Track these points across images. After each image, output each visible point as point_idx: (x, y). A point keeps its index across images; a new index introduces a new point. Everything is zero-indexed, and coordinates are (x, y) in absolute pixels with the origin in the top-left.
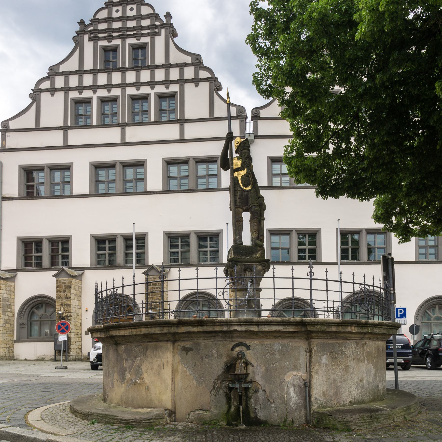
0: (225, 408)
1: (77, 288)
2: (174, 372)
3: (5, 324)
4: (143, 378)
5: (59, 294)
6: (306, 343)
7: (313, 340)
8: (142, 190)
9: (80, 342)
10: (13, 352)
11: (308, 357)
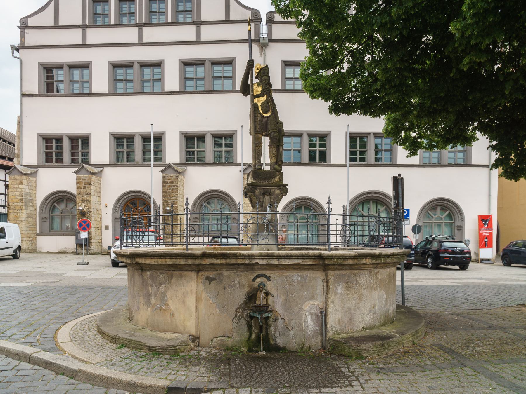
0: (246, 335)
1: (96, 184)
2: (198, 299)
3: (28, 218)
4: (168, 305)
5: (80, 190)
6: (324, 274)
7: (330, 271)
8: (160, 90)
9: (101, 237)
10: (36, 245)
11: (325, 287)
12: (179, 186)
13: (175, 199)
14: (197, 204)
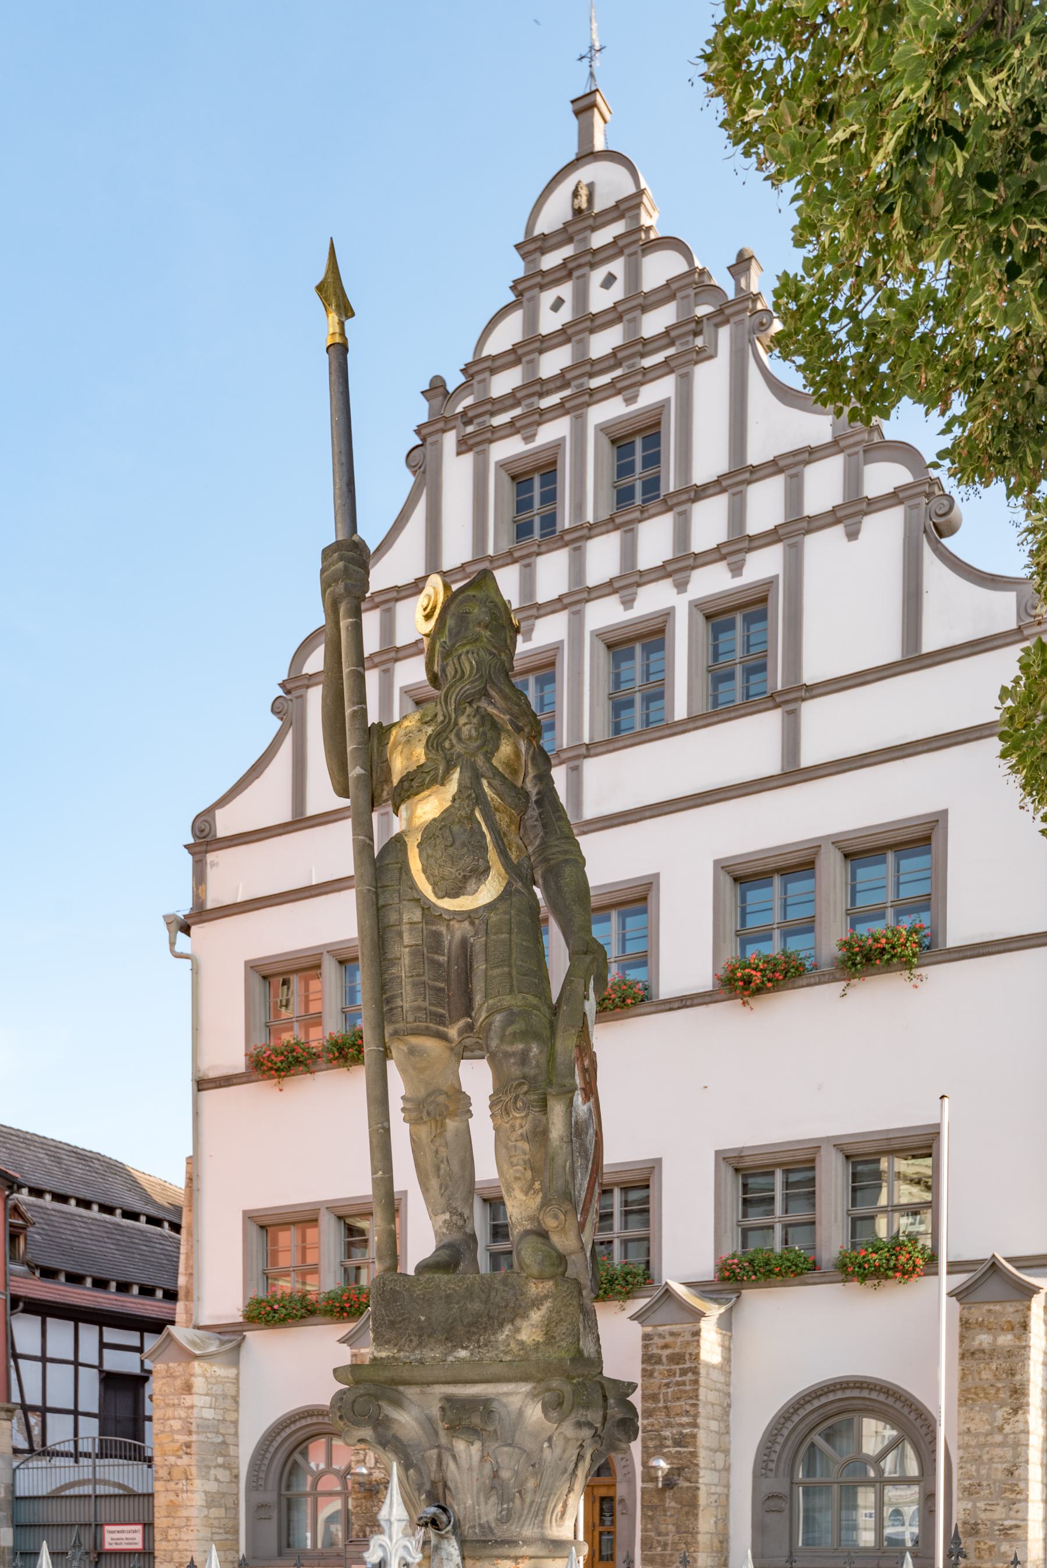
13: (689, 1425)
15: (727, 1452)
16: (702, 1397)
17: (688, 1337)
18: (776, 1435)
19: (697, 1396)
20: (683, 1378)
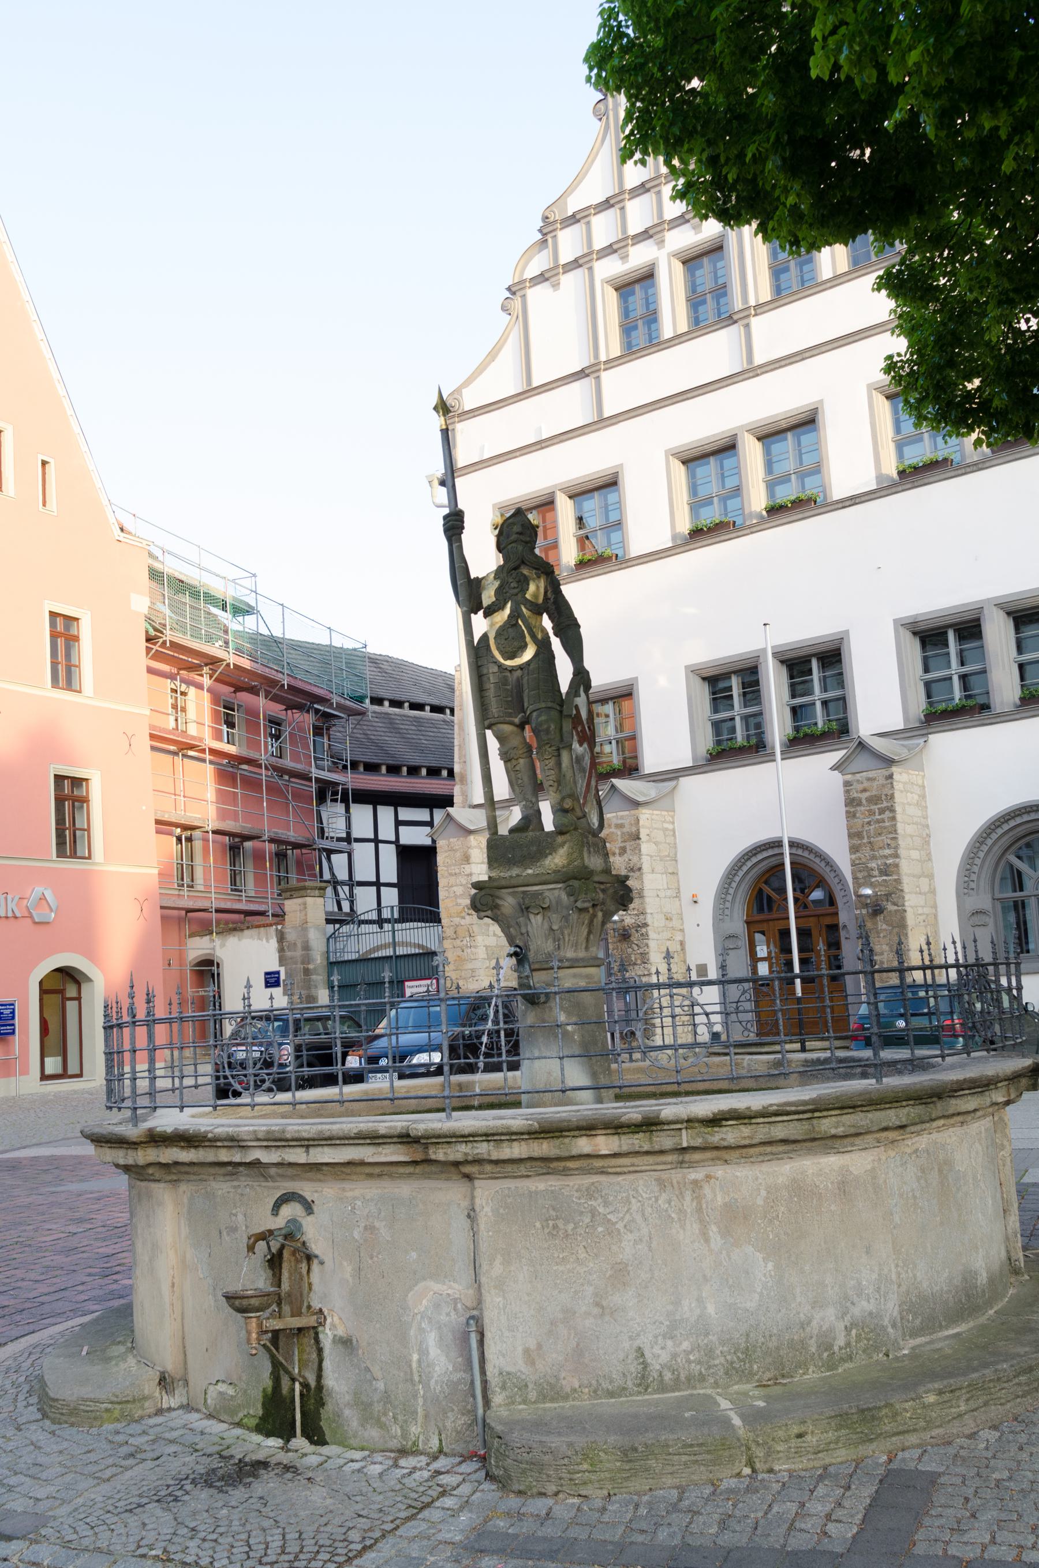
1: (659, 836)
12: (898, 809)
13: (891, 856)
14: (978, 861)
15: (931, 877)
16: (900, 831)
17: (882, 781)
18: (973, 858)
19: (895, 831)
20: (882, 816)
